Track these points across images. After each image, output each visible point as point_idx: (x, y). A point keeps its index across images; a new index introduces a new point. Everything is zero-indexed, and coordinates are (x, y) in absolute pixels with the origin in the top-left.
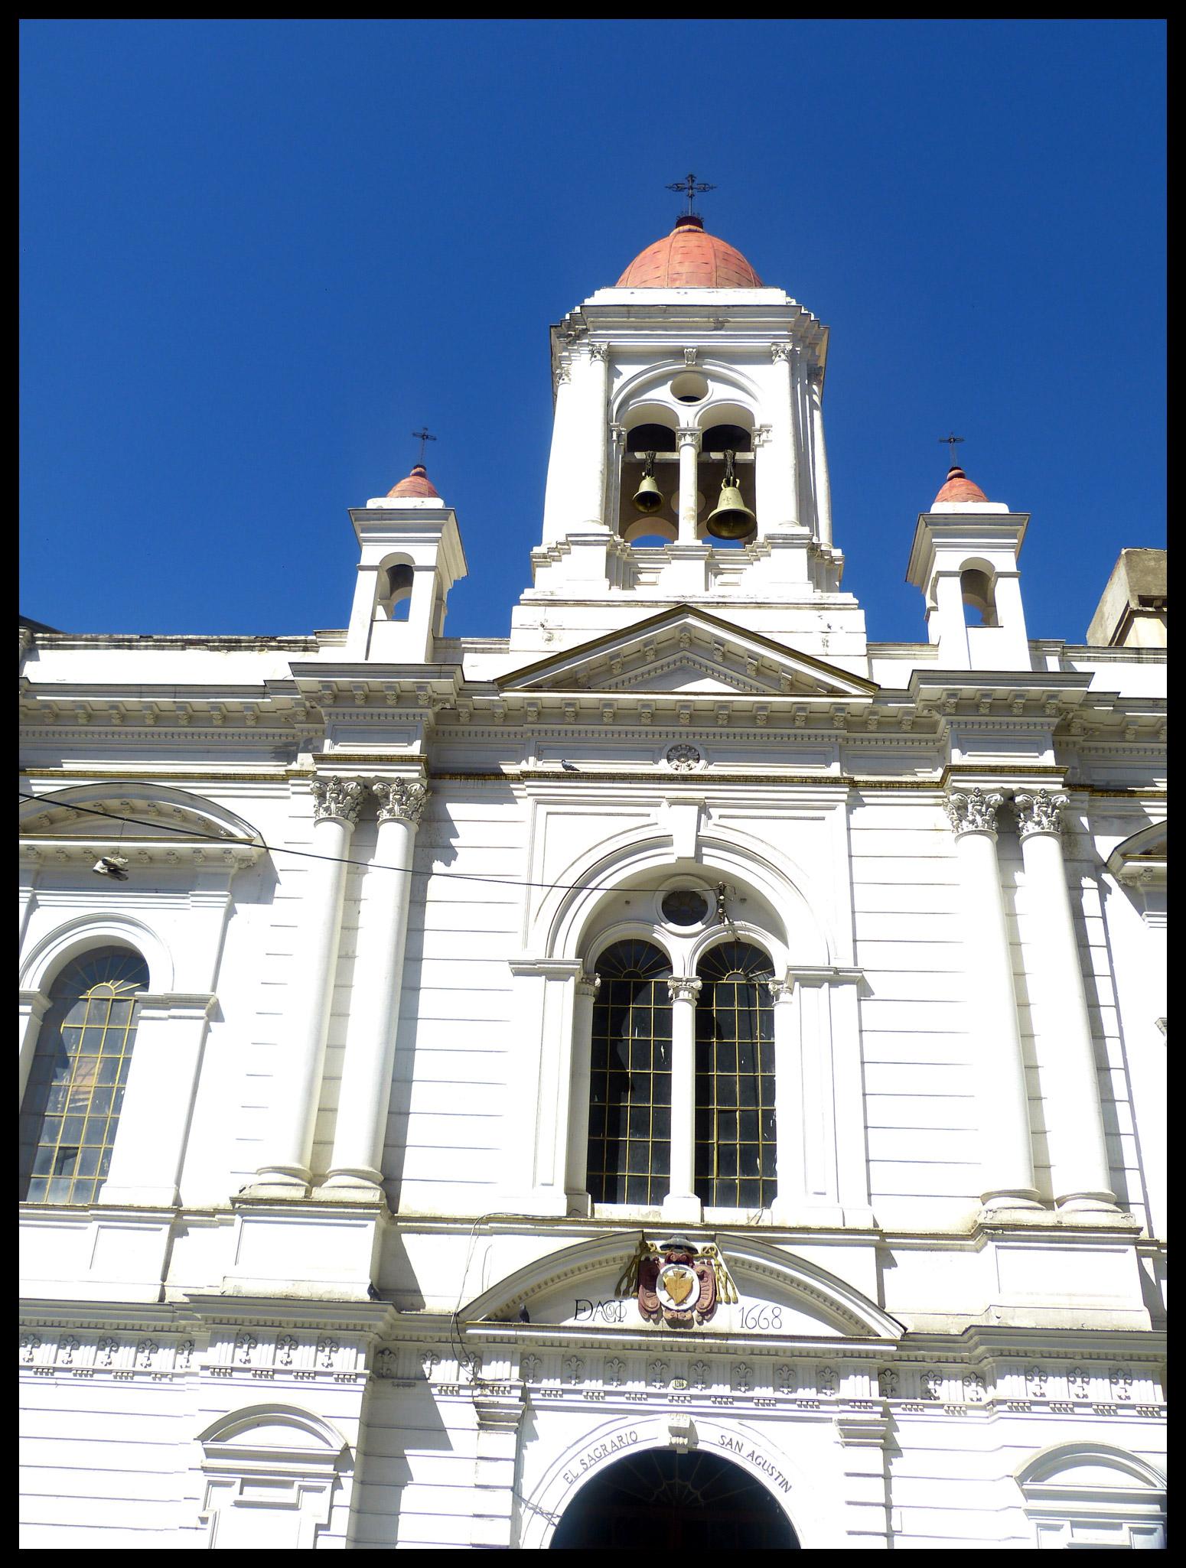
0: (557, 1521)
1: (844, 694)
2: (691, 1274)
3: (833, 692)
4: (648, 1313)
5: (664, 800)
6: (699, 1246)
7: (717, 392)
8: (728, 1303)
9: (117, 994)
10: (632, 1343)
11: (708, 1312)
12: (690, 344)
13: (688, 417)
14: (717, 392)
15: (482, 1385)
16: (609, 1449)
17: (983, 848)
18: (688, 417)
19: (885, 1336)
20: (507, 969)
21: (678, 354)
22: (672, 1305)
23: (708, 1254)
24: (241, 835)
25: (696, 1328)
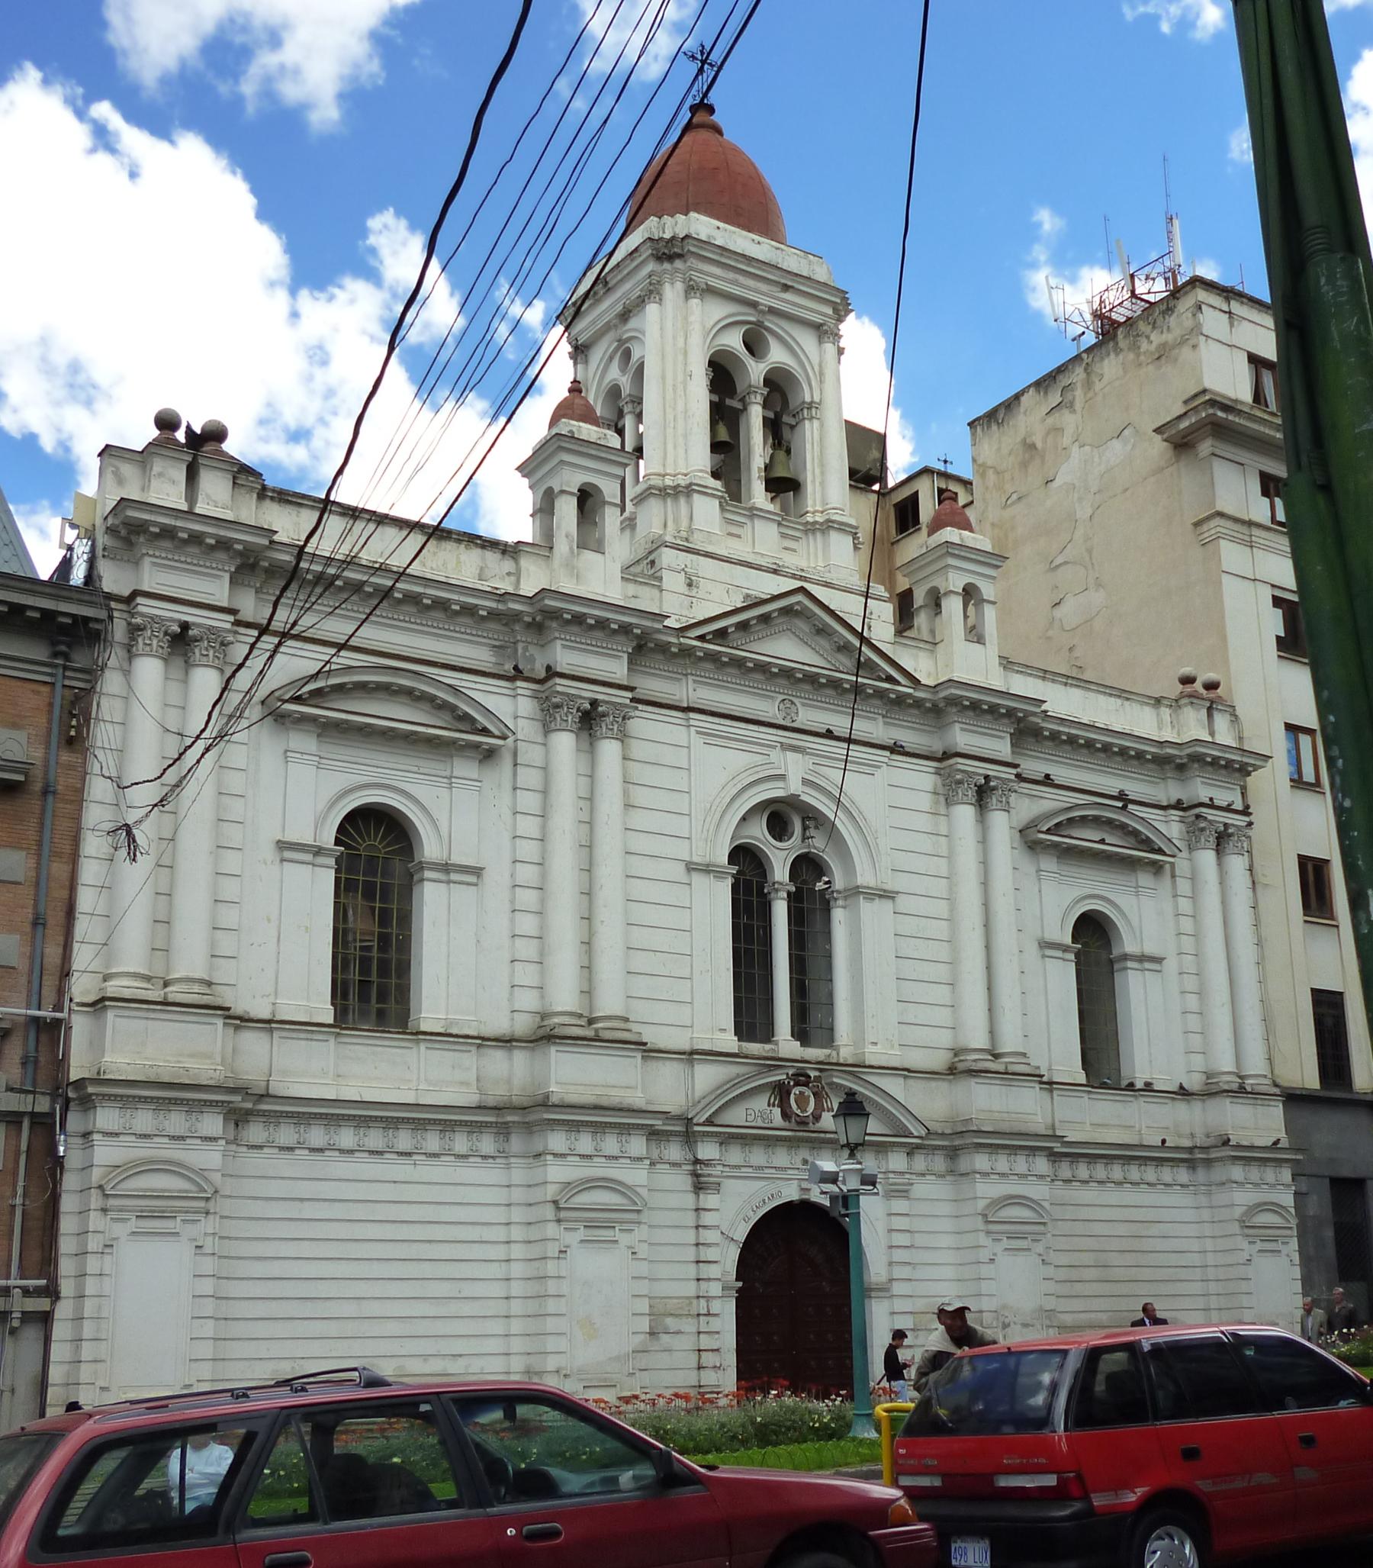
0: (741, 1245)
1: (898, 683)
2: (808, 1092)
3: (890, 679)
4: (786, 1115)
5: (779, 745)
6: (813, 1074)
7: (777, 355)
8: (828, 1111)
9: (386, 853)
10: (786, 1137)
11: (817, 1118)
12: (765, 301)
13: (756, 371)
14: (777, 355)
15: (697, 1161)
16: (767, 1201)
17: (965, 813)
18: (756, 371)
19: (916, 1134)
20: (682, 867)
21: (754, 305)
22: (798, 1112)
23: (818, 1079)
24: (497, 733)
25: (811, 1127)
